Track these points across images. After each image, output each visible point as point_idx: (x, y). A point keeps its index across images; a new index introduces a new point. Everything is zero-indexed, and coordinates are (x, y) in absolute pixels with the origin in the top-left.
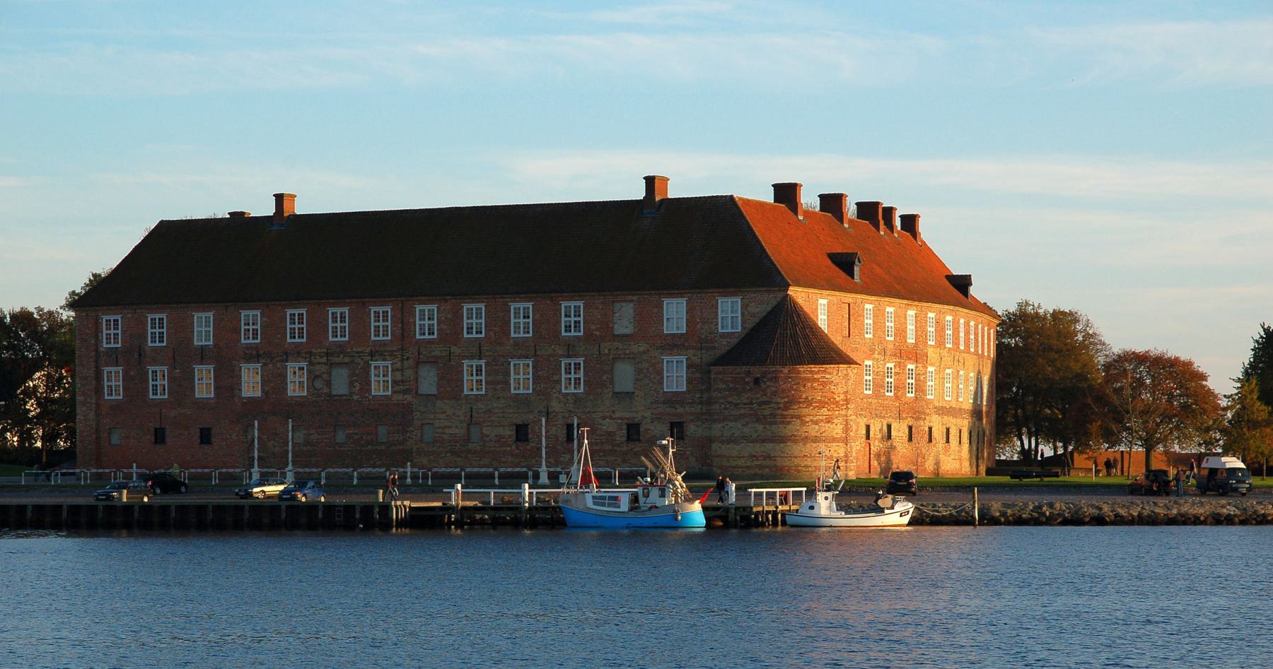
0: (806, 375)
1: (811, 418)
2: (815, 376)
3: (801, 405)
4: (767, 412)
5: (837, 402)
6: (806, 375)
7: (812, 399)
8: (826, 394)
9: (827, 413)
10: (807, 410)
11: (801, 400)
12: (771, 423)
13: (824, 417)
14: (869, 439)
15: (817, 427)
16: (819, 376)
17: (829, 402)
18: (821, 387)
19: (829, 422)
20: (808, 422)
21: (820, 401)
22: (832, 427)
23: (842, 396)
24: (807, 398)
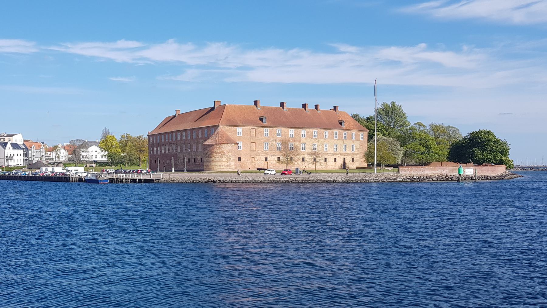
4: (208, 155)
12: (208, 158)
14: (267, 161)
15: (218, 158)
23: (226, 151)
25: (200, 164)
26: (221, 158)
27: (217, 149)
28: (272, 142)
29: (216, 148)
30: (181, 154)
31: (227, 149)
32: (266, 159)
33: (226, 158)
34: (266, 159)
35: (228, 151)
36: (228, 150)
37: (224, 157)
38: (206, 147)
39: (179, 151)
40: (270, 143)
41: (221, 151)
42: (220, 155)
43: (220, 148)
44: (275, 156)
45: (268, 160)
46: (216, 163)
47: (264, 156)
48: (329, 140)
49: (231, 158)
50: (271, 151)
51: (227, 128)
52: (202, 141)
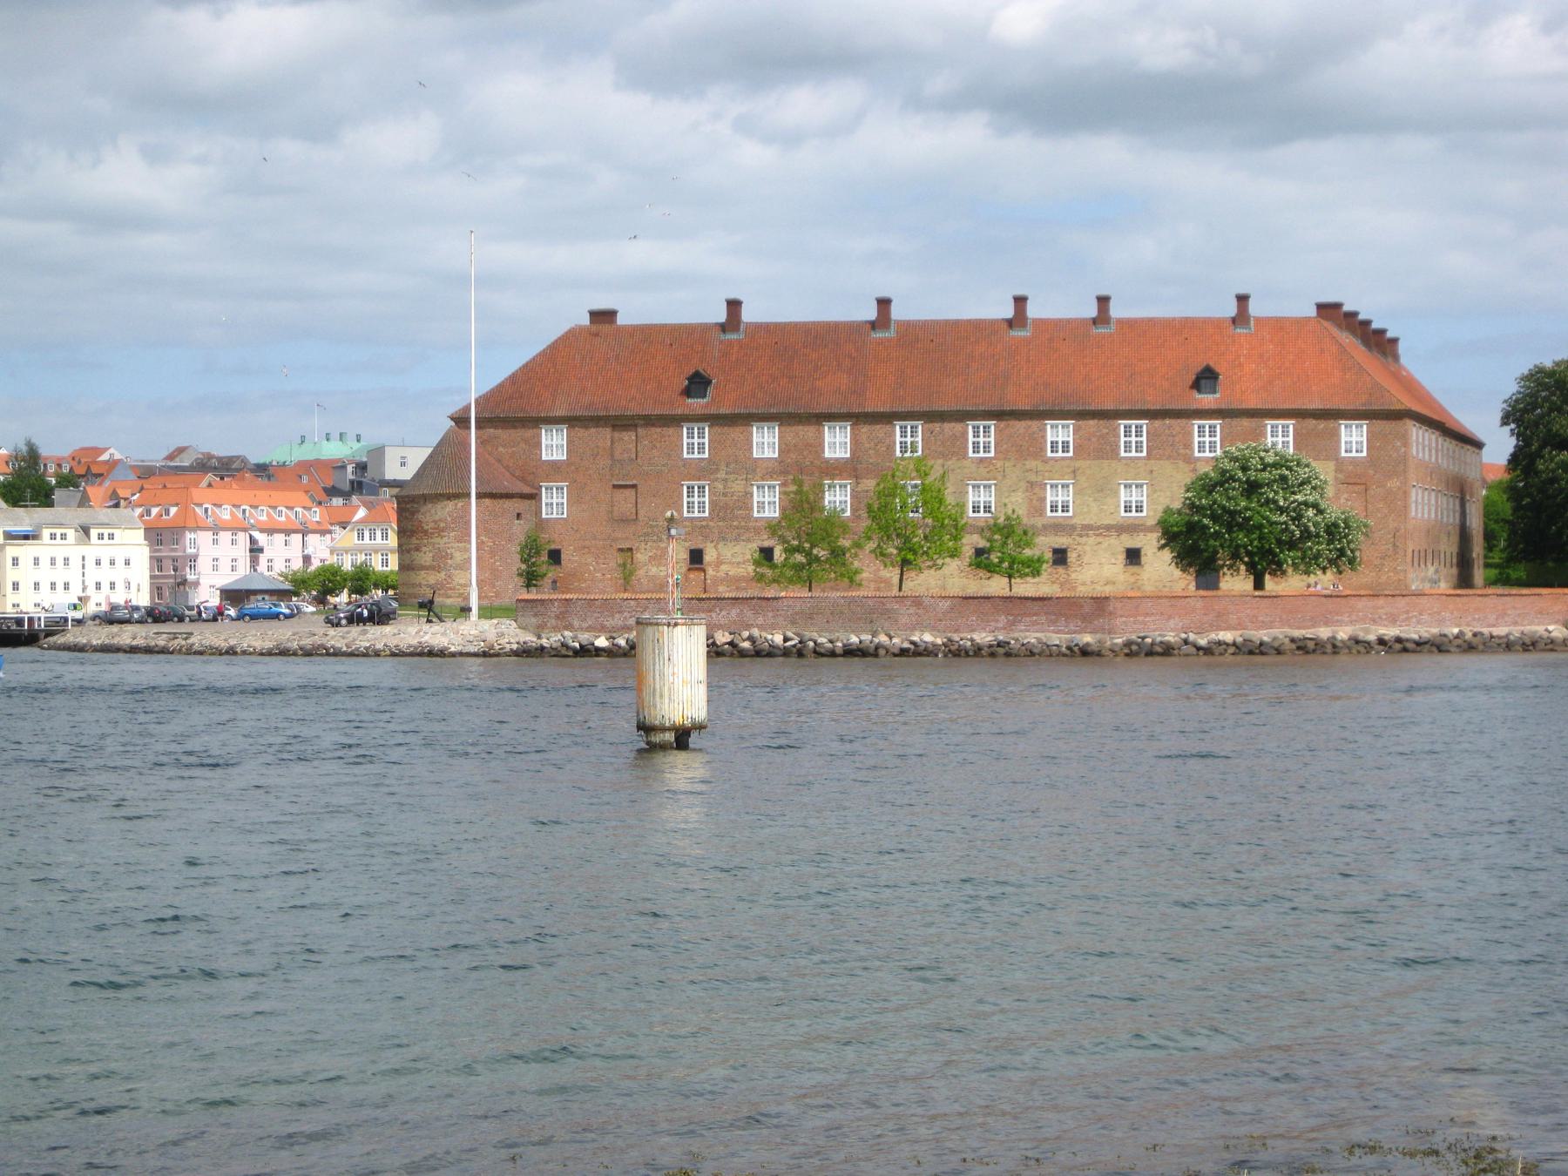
23: (432, 525)
28: (725, 480)
31: (437, 518)
32: (696, 557)
34: (696, 557)
35: (442, 525)
36: (440, 520)
40: (720, 486)
44: (748, 540)
45: (707, 558)
47: (687, 544)
48: (1078, 464)
50: (724, 520)
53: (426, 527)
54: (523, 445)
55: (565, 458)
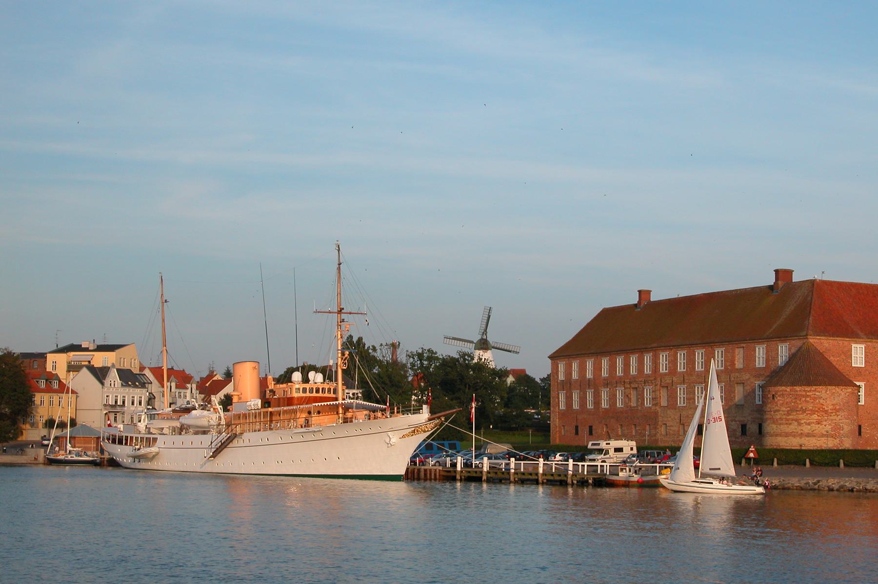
0: (801, 393)
1: (805, 421)
2: (808, 394)
3: (798, 412)
4: (778, 417)
5: (826, 411)
6: (801, 393)
7: (806, 409)
8: (816, 406)
9: (817, 417)
10: (802, 415)
11: (797, 409)
12: (780, 424)
13: (815, 421)
15: (809, 427)
16: (811, 394)
17: (819, 410)
18: (813, 401)
19: (818, 424)
20: (802, 424)
21: (811, 410)
22: (821, 427)
23: (831, 407)
24: (802, 408)
25: (740, 440)
26: (817, 426)
27: (806, 401)
29: (804, 399)
30: (670, 412)
31: (835, 402)
33: (830, 425)
36: (837, 404)
37: (824, 423)
38: (773, 395)
39: (664, 403)
41: (819, 406)
42: (815, 417)
43: (814, 399)
46: (803, 439)
49: (845, 427)
51: (827, 345)
52: (747, 377)
53: (826, 409)
54: (843, 356)
55: (864, 366)
